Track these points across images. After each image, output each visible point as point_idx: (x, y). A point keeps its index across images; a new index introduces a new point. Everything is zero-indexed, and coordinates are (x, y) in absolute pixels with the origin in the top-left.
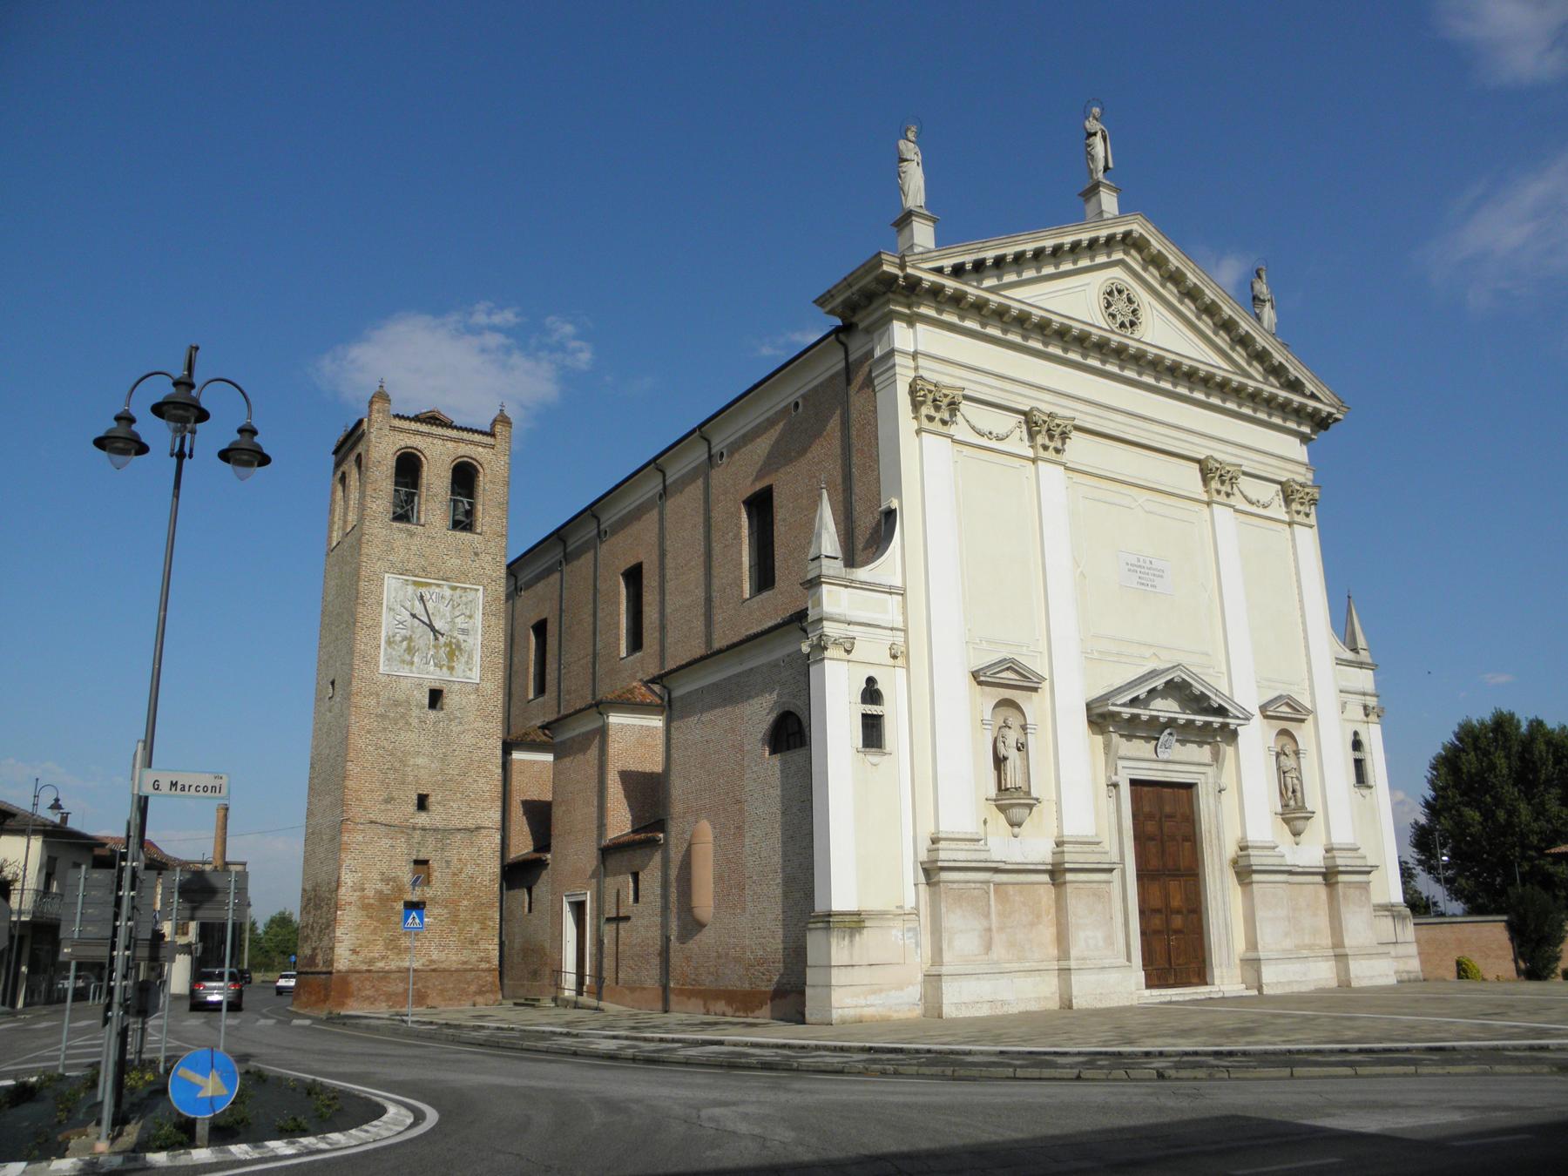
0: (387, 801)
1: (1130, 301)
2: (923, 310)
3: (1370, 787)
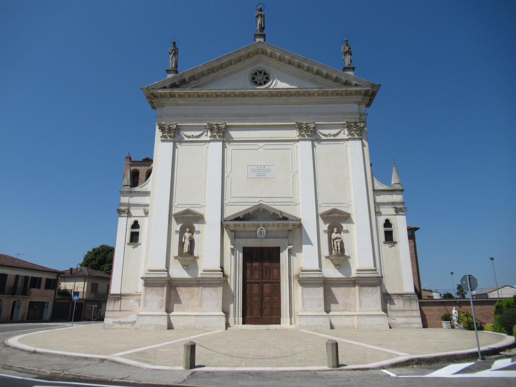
3: (396, 243)
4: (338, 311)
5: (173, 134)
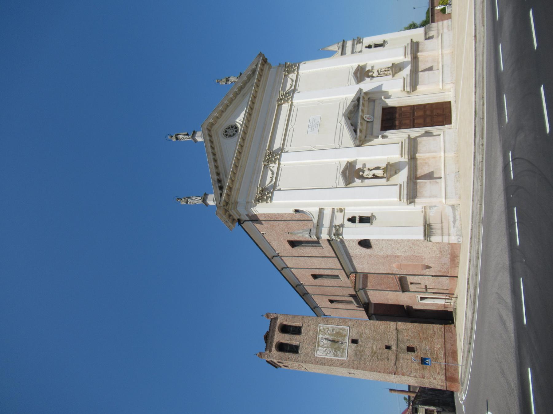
0: (388, 359)
1: (229, 128)
3: (384, 41)
4: (438, 65)
5: (265, 194)
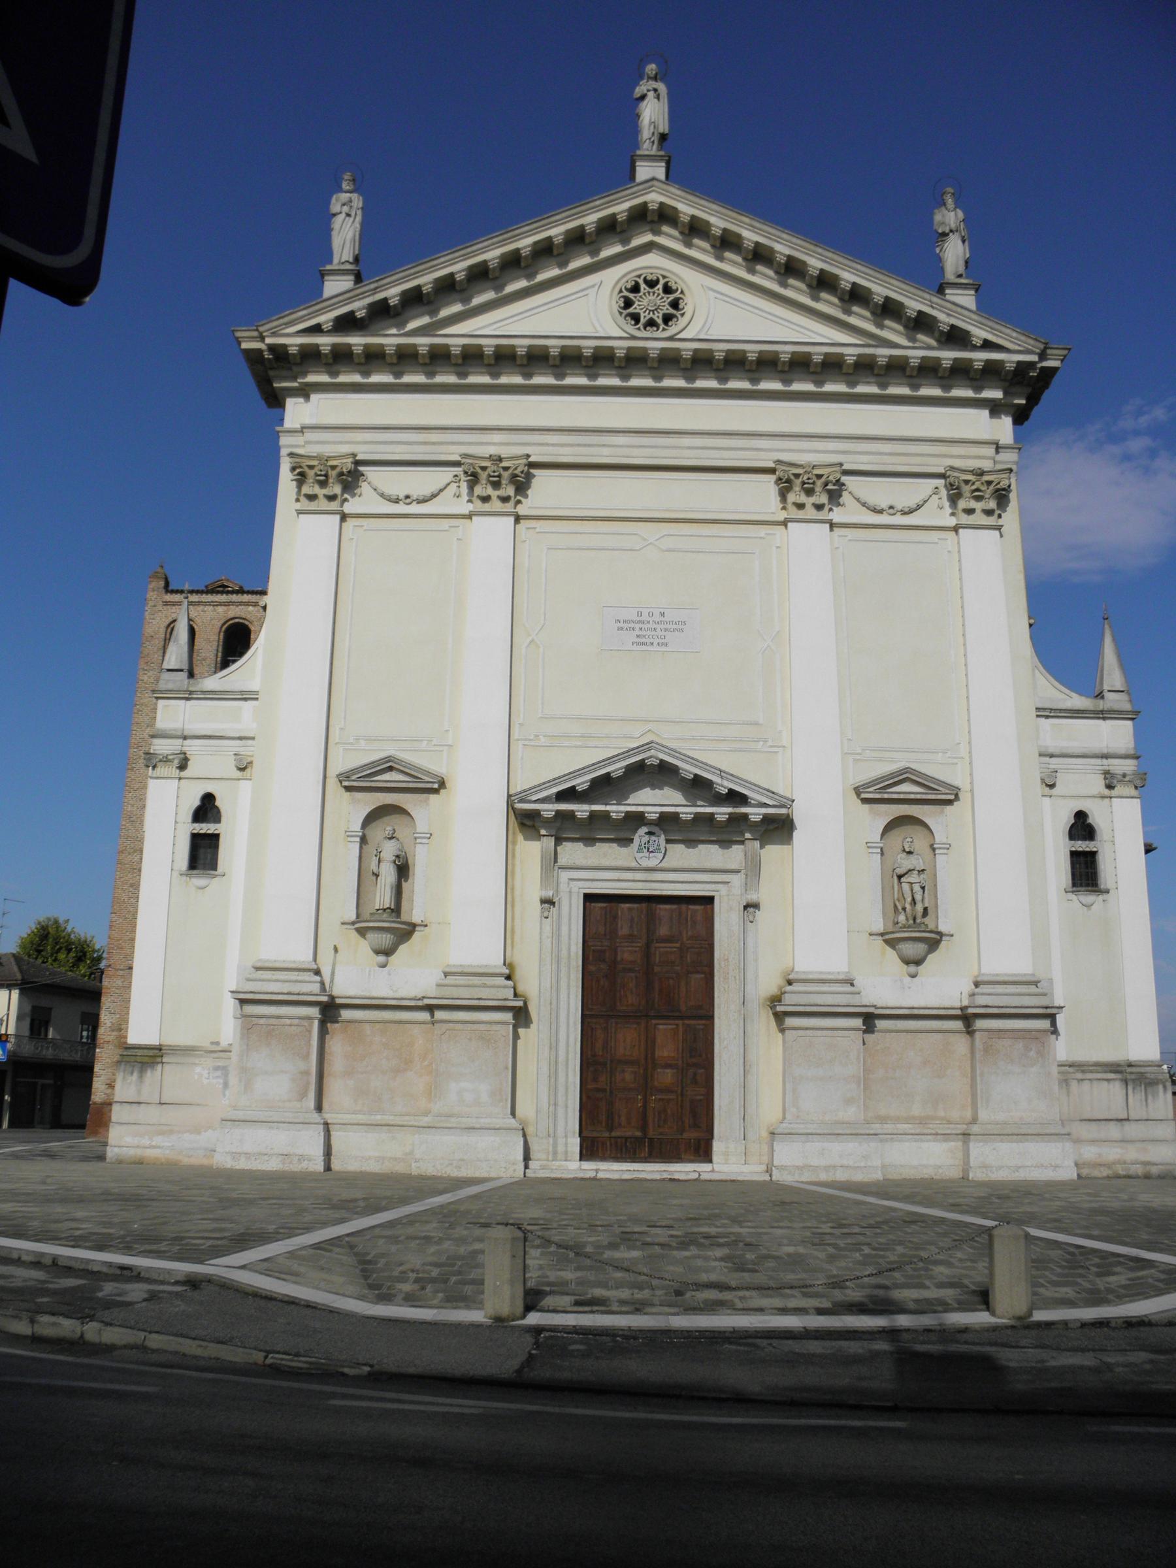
2: (312, 378)
